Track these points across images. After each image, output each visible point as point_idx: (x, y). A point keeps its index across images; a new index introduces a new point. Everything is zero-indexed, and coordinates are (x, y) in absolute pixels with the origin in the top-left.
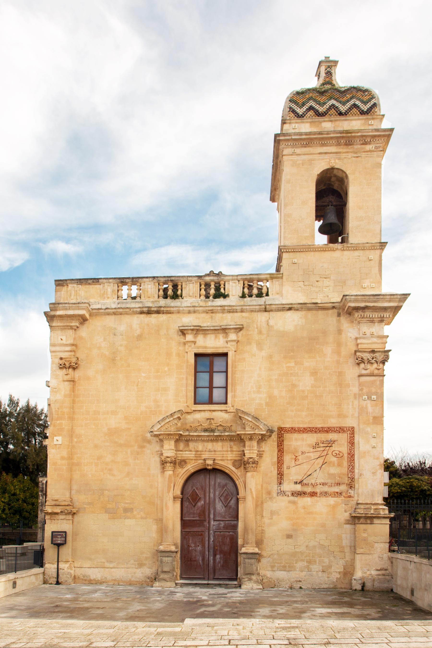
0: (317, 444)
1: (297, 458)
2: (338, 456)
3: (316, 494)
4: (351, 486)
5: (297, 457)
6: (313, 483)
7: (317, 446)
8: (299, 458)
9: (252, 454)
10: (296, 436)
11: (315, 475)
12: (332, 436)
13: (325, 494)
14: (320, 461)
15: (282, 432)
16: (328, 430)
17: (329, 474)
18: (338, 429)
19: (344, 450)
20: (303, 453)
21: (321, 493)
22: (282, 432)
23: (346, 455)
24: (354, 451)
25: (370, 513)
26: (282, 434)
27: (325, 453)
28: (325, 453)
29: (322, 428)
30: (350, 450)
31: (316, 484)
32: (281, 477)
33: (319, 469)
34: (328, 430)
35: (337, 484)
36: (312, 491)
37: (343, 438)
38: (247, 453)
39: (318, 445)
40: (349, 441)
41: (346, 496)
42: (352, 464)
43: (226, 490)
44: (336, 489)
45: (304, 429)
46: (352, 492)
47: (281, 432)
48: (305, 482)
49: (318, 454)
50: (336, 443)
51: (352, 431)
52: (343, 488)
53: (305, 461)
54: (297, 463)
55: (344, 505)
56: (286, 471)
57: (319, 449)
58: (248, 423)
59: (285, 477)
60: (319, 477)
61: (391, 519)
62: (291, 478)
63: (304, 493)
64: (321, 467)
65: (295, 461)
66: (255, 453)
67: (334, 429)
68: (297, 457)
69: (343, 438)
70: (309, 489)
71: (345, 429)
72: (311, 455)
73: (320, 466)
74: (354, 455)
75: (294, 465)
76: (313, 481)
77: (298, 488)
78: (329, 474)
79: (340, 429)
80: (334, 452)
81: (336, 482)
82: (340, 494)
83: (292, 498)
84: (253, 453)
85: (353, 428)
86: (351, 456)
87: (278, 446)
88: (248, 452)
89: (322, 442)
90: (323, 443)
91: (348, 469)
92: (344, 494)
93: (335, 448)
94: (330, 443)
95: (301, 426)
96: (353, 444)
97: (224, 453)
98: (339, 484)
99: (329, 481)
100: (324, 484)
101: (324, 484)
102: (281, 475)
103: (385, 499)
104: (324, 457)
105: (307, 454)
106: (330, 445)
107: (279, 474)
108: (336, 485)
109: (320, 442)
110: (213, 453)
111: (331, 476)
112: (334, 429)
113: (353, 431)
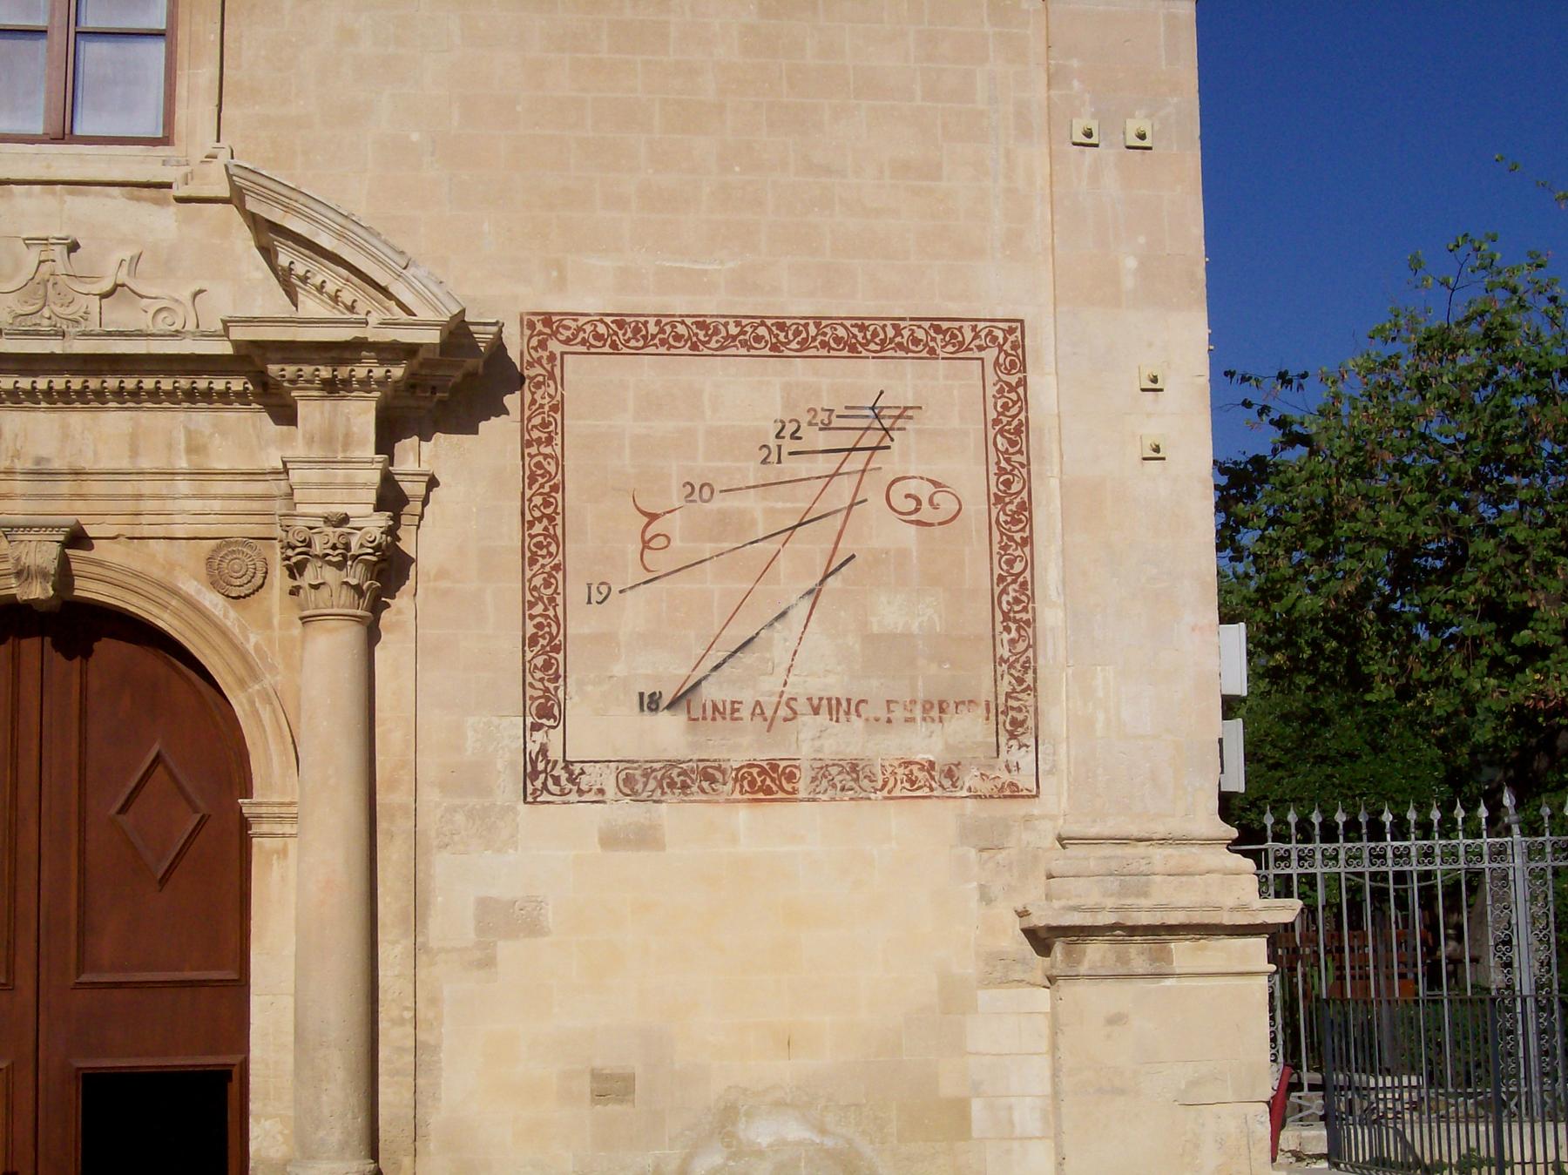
0: (789, 431)
1: (654, 528)
2: (926, 513)
3: (791, 777)
4: (1015, 720)
5: (653, 517)
6: (769, 703)
7: (788, 445)
8: (672, 525)
9: (340, 495)
11: (781, 641)
12: (897, 380)
13: (849, 778)
14: (812, 547)
15: (555, 346)
16: (858, 339)
17: (869, 639)
18: (920, 334)
19: (969, 476)
20: (695, 491)
21: (822, 772)
22: (555, 346)
24: (1027, 483)
25: (1144, 902)
26: (552, 357)
27: (843, 490)
28: (843, 490)
29: (818, 320)
30: (1002, 471)
31: (783, 712)
32: (547, 665)
33: (806, 605)
34: (858, 339)
35: (927, 706)
36: (762, 756)
37: (951, 394)
38: (306, 485)
39: (794, 436)
40: (992, 415)
41: (985, 787)
42: (1018, 567)
43: (158, 759)
45: (702, 325)
46: (1026, 759)
47: (542, 345)
48: (712, 692)
50: (910, 425)
51: (1008, 346)
52: (970, 728)
53: (708, 549)
54: (659, 561)
55: (973, 852)
56: (581, 623)
57: (801, 467)
58: (314, 267)
59: (577, 663)
60: (813, 658)
61: (1277, 936)
62: (619, 669)
63: (709, 775)
64: (814, 594)
65: (646, 545)
66: (1511, 442)
67: (898, 333)
68: (653, 517)
69: (951, 394)
70: (741, 747)
71: (969, 335)
72: (752, 503)
73: (811, 583)
74: (1025, 507)
75: (634, 574)
76: (768, 687)
77: (668, 736)
78: (869, 639)
79: (938, 330)
80: (898, 492)
81: (921, 696)
82: (949, 774)
83: (625, 812)
84: (350, 485)
85: (1016, 325)
86: (1013, 514)
87: (527, 444)
88: (314, 475)
89: (823, 416)
90: (826, 427)
91: (995, 602)
92: (970, 779)
93: (905, 457)
94: (883, 423)
95: (680, 304)
96: (1018, 431)
97: (147, 487)
98: (938, 709)
99: (873, 688)
100: (836, 708)
101: (836, 708)
102: (545, 647)
103: (1228, 806)
104: (840, 517)
105: (719, 503)
106: (871, 439)
107: (534, 640)
108: (918, 713)
109: (805, 419)
110: (64, 487)
111: (885, 648)
112: (898, 333)
113: (1019, 346)
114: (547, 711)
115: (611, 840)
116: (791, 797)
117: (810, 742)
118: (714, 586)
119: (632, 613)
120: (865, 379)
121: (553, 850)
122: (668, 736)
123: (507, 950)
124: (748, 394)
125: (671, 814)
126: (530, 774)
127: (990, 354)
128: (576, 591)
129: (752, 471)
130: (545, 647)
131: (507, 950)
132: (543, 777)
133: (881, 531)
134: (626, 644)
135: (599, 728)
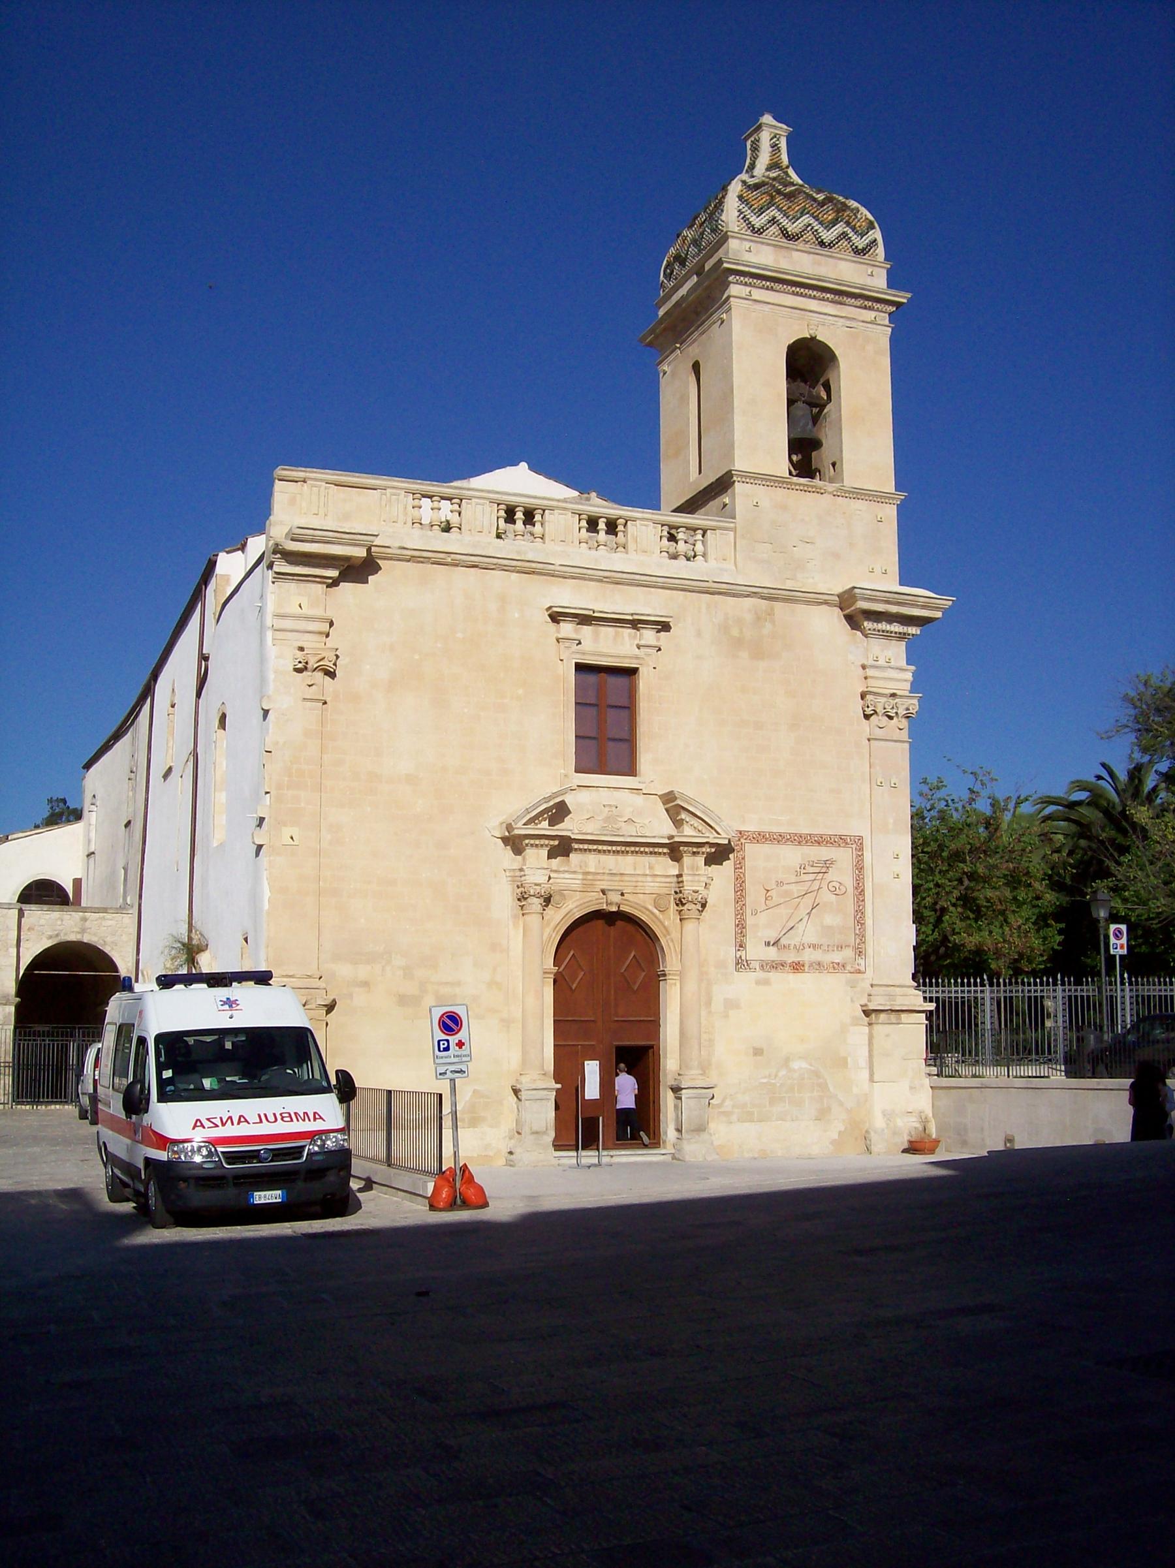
4: (860, 952)
8: (773, 893)
10: (766, 848)
11: (801, 926)
13: (819, 966)
14: (808, 901)
15: (743, 841)
16: (819, 841)
19: (849, 883)
20: (780, 883)
22: (743, 841)
23: (850, 890)
27: (816, 885)
28: (816, 885)
34: (819, 841)
36: (796, 960)
37: (843, 857)
44: (837, 957)
48: (783, 941)
49: (803, 888)
51: (859, 843)
52: (849, 953)
53: (782, 900)
56: (750, 921)
60: (808, 932)
64: (809, 914)
69: (843, 857)
70: (791, 957)
72: (793, 887)
74: (863, 890)
77: (772, 954)
83: (760, 974)
85: (861, 838)
86: (860, 892)
88: (690, 878)
92: (848, 968)
93: (832, 875)
94: (828, 864)
97: (640, 879)
98: (840, 947)
100: (814, 946)
101: (814, 946)
102: (741, 926)
105: (785, 887)
110: (617, 878)
114: (742, 946)
115: (758, 983)
116: (804, 971)
117: (808, 956)
118: (784, 911)
119: (763, 918)
120: (825, 853)
121: (743, 985)
122: (772, 954)
123: (731, 1012)
124: (792, 856)
125: (773, 976)
126: (737, 964)
127: (854, 846)
128: (749, 912)
129: (793, 879)
130: (741, 926)
131: (731, 1012)
132: (741, 964)
133: (826, 897)
134: (762, 927)
135: (755, 951)
